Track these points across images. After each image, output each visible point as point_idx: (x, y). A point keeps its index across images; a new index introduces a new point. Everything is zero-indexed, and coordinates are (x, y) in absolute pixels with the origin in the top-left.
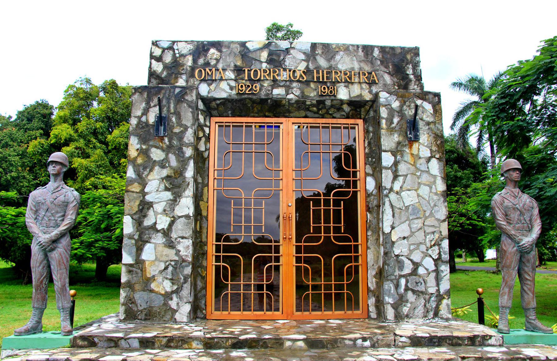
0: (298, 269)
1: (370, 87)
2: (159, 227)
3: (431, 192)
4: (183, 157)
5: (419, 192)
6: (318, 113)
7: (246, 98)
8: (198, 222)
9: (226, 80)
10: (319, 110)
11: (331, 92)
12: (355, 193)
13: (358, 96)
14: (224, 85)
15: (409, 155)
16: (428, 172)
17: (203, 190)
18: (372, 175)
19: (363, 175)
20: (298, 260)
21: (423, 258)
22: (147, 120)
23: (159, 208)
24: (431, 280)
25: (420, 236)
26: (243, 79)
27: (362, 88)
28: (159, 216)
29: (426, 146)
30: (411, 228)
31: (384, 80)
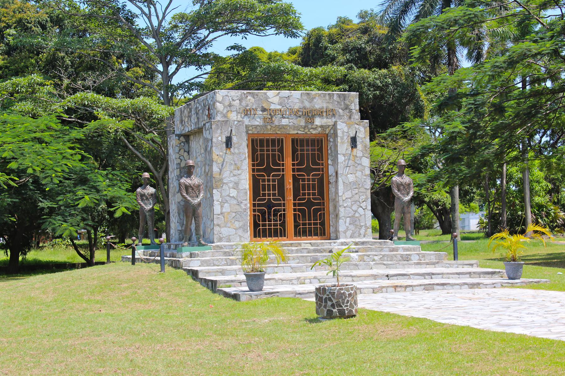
0: (295, 215)
2: (231, 195)
18: (332, 165)
20: (295, 210)
23: (231, 185)
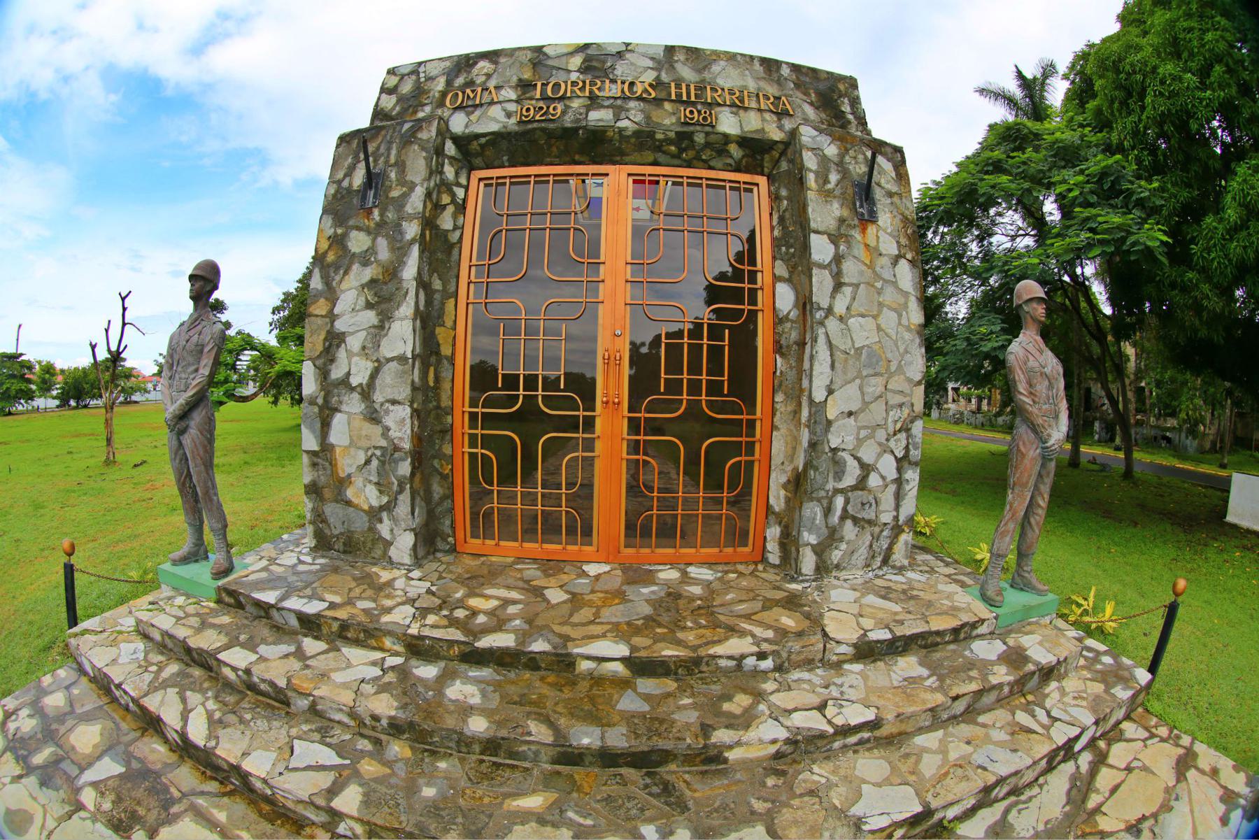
1: (779, 120)
3: (900, 324)
4: (401, 241)
5: (880, 320)
6: (678, 156)
7: (535, 129)
8: (432, 369)
9: (500, 102)
10: (681, 150)
11: (705, 119)
12: (753, 315)
13: (757, 131)
14: (496, 111)
15: (862, 247)
16: (894, 284)
17: (443, 304)
18: (789, 281)
19: (768, 279)
20: (635, 447)
21: (879, 456)
22: (351, 184)
24: (888, 498)
25: (878, 409)
26: (531, 99)
27: (763, 120)
28: (355, 359)
29: (890, 234)
30: (863, 394)
31: (804, 112)
